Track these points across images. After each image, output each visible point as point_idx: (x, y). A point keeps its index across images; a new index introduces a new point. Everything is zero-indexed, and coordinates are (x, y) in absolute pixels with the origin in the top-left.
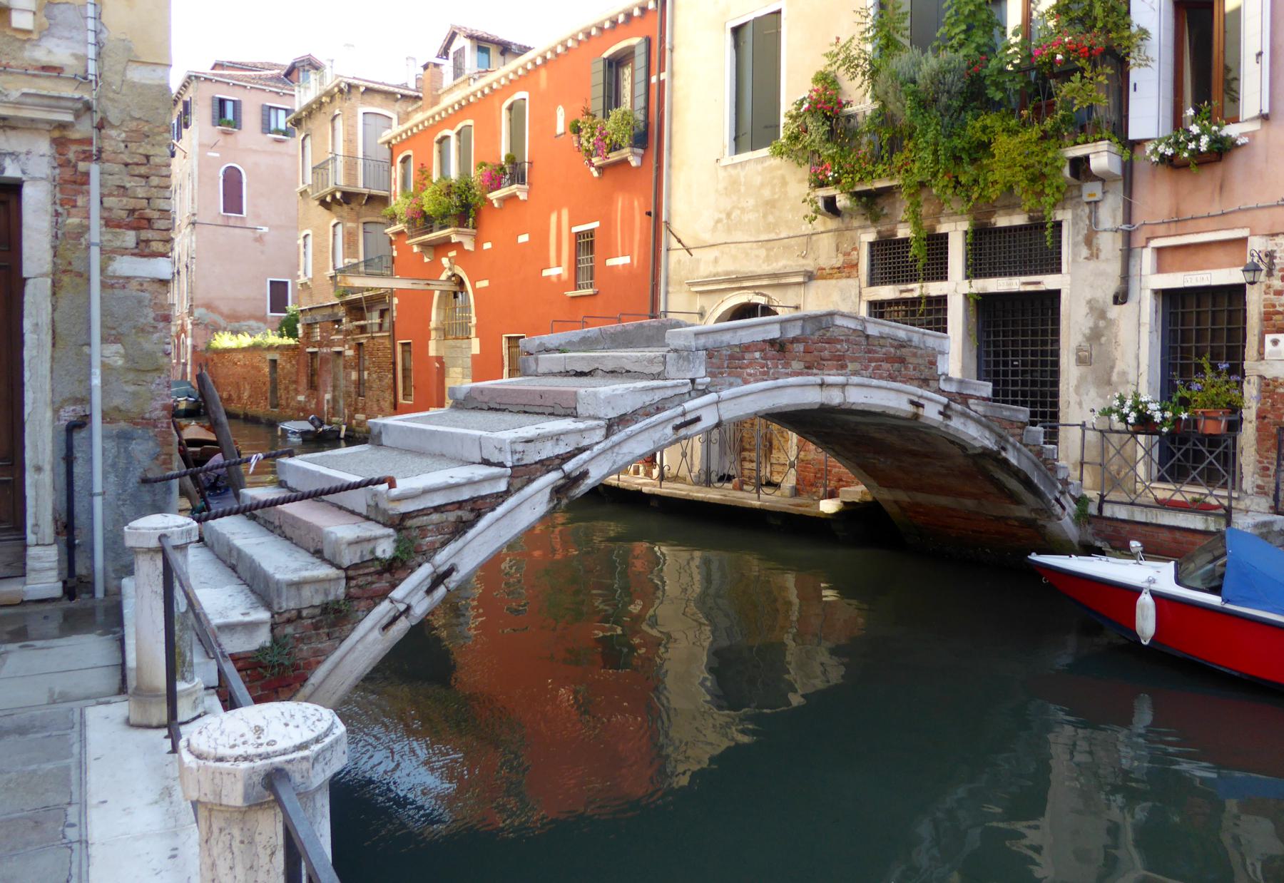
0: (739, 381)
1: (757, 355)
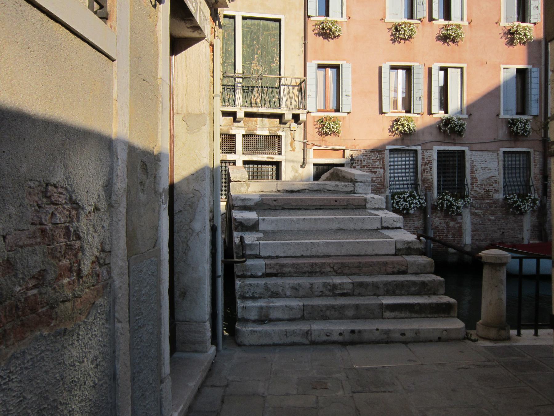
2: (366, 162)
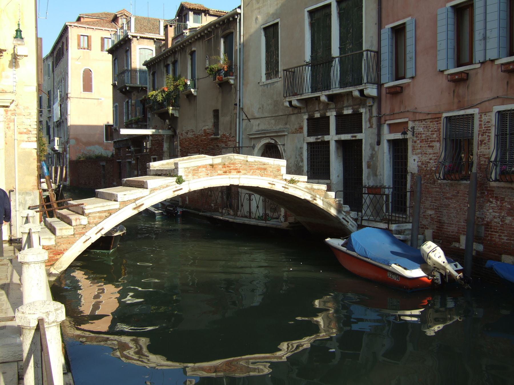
0: (197, 177)
1: (204, 169)
2: (425, 135)
